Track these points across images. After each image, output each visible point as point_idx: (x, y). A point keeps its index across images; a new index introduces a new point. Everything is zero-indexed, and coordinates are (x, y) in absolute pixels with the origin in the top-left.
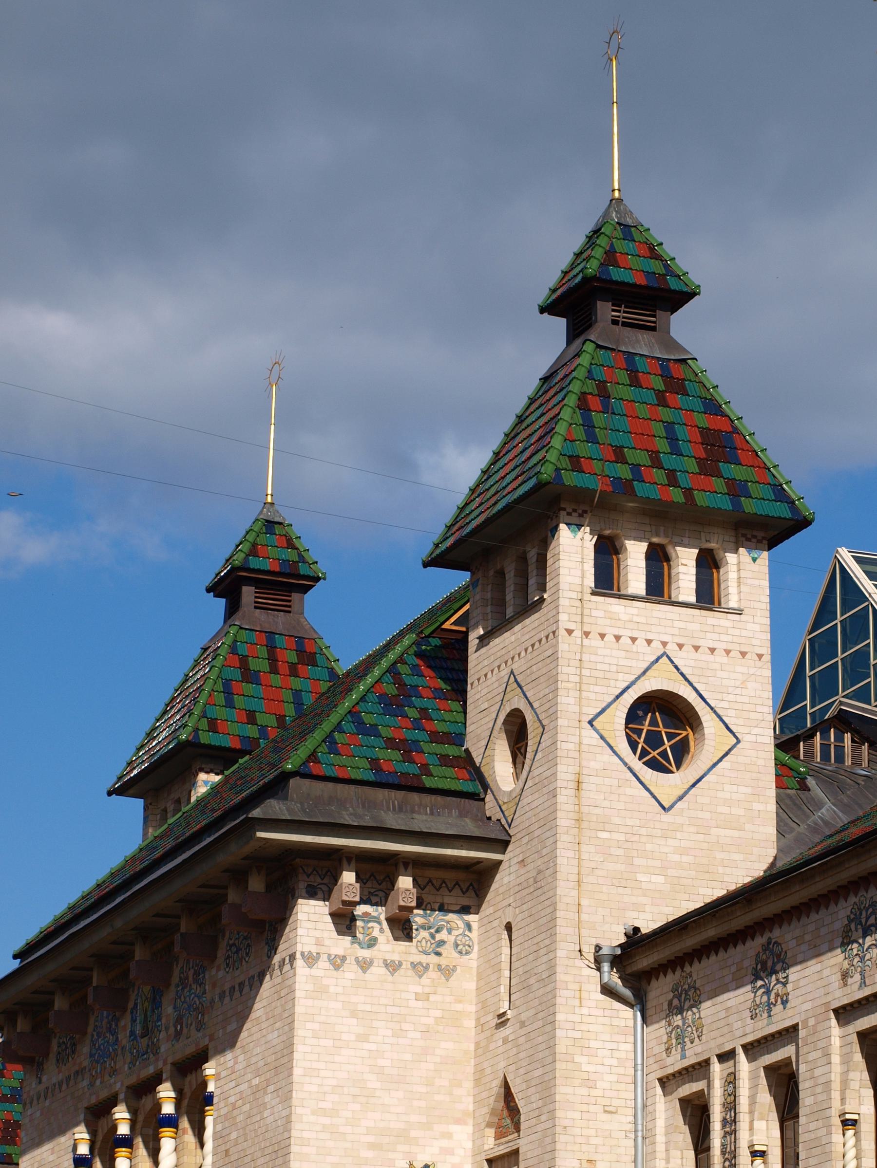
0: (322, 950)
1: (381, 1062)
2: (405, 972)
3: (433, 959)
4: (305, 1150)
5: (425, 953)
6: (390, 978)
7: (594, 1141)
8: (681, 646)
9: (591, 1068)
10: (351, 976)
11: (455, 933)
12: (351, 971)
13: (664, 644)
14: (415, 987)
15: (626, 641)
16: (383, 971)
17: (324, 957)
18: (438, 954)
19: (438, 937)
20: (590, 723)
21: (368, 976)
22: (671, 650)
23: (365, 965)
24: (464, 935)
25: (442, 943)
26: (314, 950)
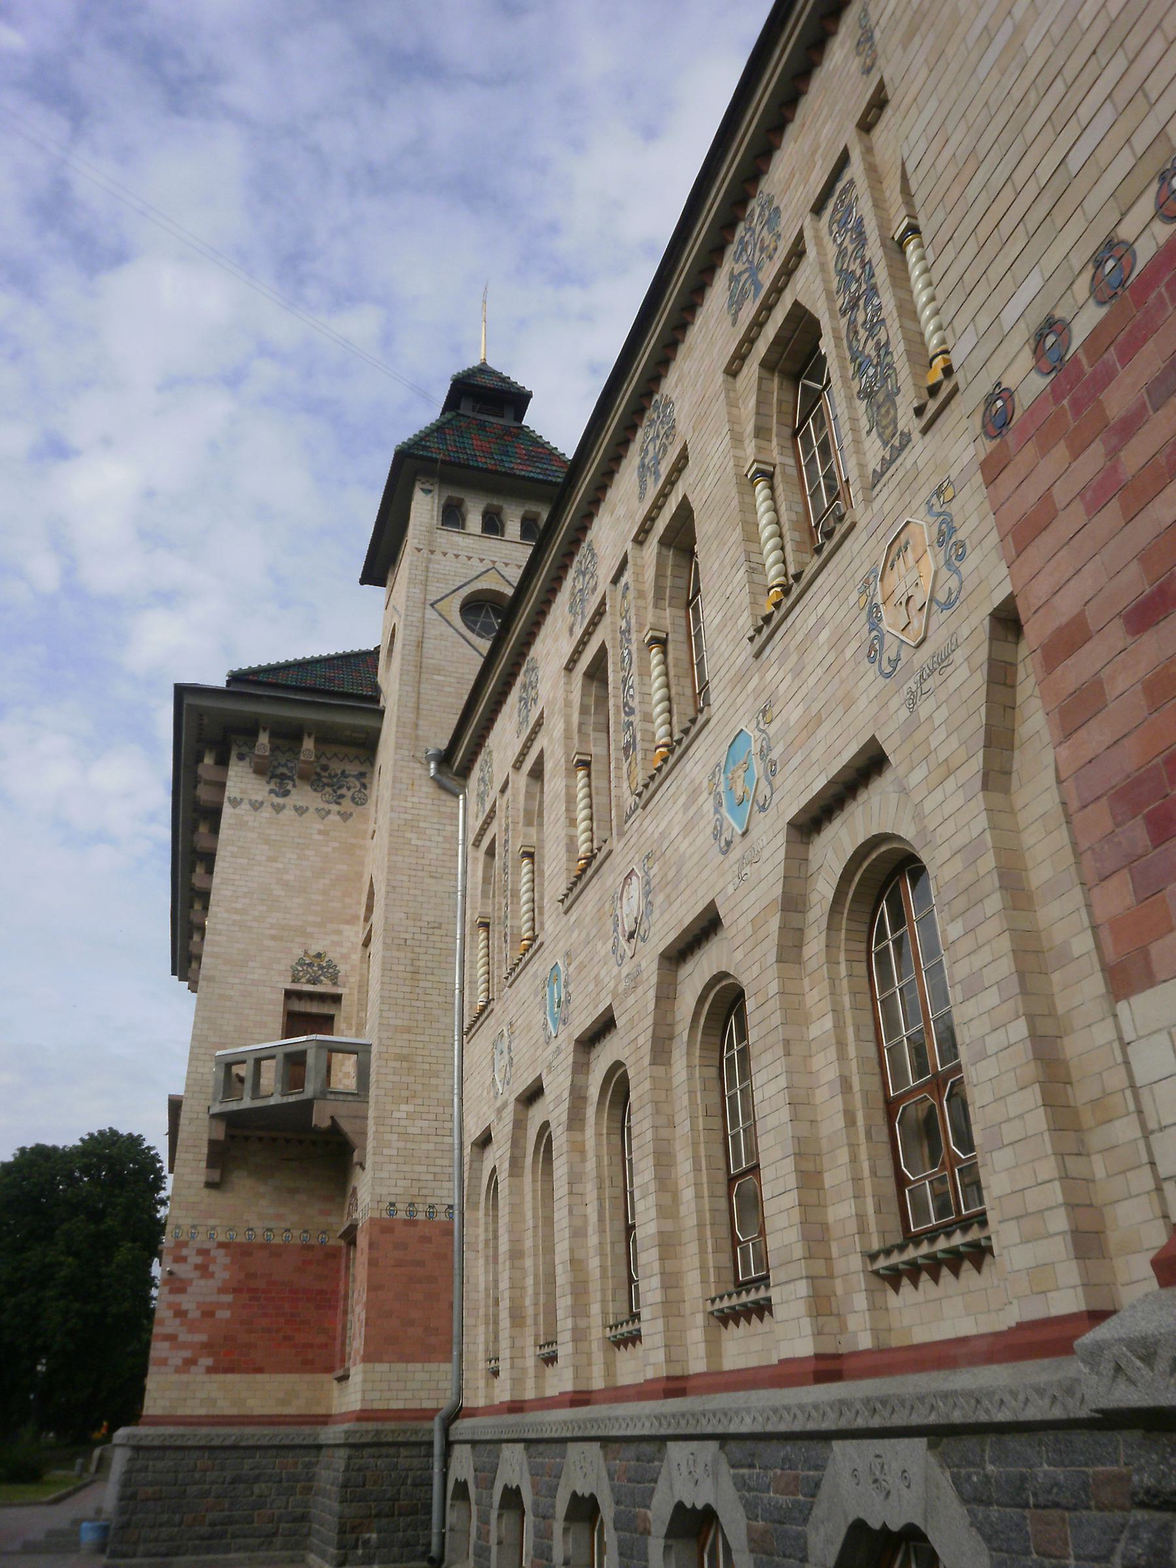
0: (245, 796)
1: (286, 877)
2: (311, 815)
3: (335, 808)
4: (217, 938)
5: (328, 802)
6: (298, 818)
7: (420, 899)
8: (506, 565)
9: (420, 843)
10: (267, 815)
11: (352, 790)
12: (266, 813)
13: (494, 562)
14: (318, 826)
15: (463, 559)
16: (293, 813)
17: (246, 801)
18: (339, 804)
19: (339, 792)
20: (432, 605)
21: (280, 816)
22: (499, 566)
23: (278, 809)
24: (360, 791)
25: (342, 796)
26: (239, 797)
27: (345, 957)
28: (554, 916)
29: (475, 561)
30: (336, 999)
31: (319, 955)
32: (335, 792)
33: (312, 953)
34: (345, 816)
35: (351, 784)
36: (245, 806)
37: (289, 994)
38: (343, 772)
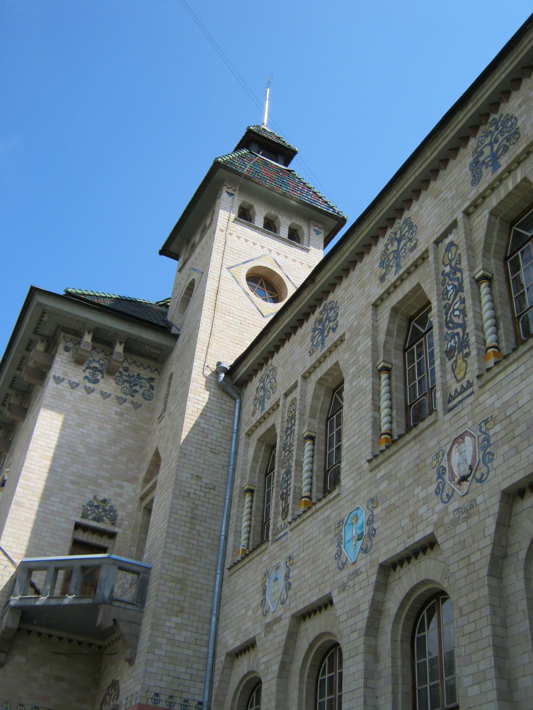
0: (66, 377)
1: (88, 440)
3: (129, 398)
4: (30, 475)
5: (125, 393)
6: (102, 400)
7: (202, 466)
9: (206, 427)
10: (80, 394)
11: (144, 389)
12: (80, 392)
16: (99, 396)
18: (133, 396)
19: (134, 388)
20: (228, 269)
21: (90, 396)
23: (89, 391)
24: (148, 390)
25: (136, 391)
26: (61, 376)
27: (123, 506)
28: (354, 474)
29: (258, 247)
30: (112, 535)
31: (104, 501)
32: (131, 387)
33: (100, 498)
34: (136, 406)
35: (143, 384)
36: (65, 384)
37: (78, 526)
38: (139, 375)
